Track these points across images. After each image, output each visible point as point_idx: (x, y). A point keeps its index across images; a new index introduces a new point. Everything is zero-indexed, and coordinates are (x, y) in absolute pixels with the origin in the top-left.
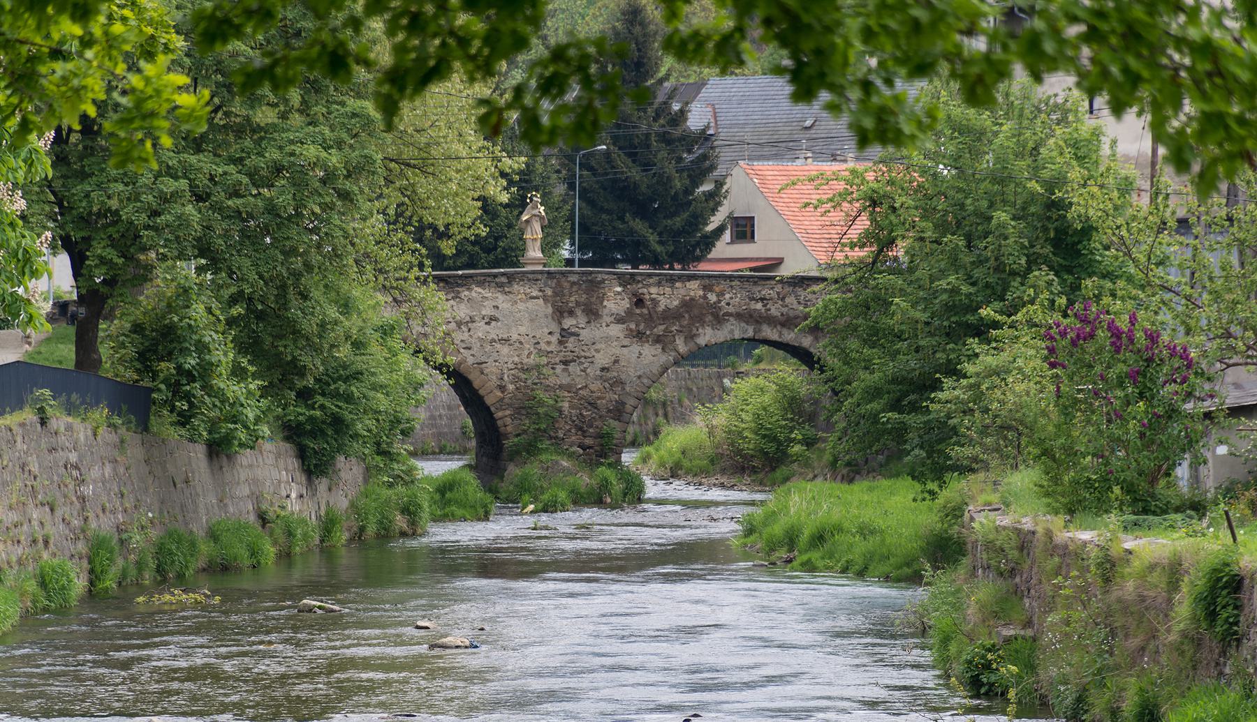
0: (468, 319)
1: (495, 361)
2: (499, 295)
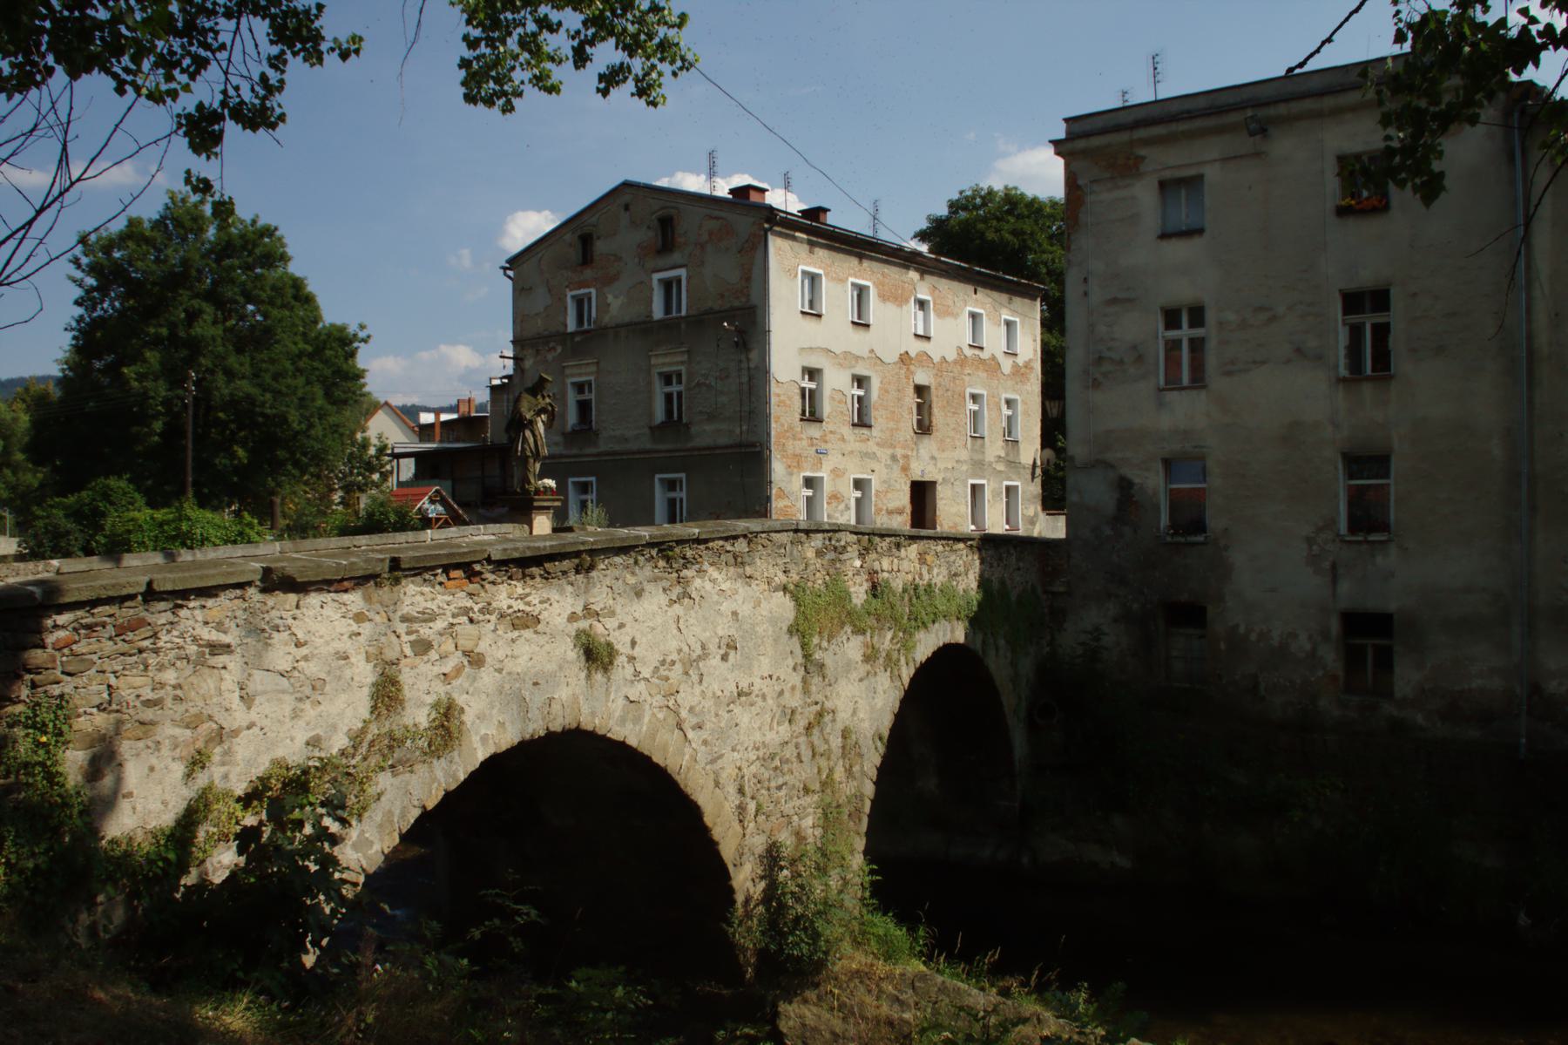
0: (699, 651)
1: (733, 750)
2: (739, 584)
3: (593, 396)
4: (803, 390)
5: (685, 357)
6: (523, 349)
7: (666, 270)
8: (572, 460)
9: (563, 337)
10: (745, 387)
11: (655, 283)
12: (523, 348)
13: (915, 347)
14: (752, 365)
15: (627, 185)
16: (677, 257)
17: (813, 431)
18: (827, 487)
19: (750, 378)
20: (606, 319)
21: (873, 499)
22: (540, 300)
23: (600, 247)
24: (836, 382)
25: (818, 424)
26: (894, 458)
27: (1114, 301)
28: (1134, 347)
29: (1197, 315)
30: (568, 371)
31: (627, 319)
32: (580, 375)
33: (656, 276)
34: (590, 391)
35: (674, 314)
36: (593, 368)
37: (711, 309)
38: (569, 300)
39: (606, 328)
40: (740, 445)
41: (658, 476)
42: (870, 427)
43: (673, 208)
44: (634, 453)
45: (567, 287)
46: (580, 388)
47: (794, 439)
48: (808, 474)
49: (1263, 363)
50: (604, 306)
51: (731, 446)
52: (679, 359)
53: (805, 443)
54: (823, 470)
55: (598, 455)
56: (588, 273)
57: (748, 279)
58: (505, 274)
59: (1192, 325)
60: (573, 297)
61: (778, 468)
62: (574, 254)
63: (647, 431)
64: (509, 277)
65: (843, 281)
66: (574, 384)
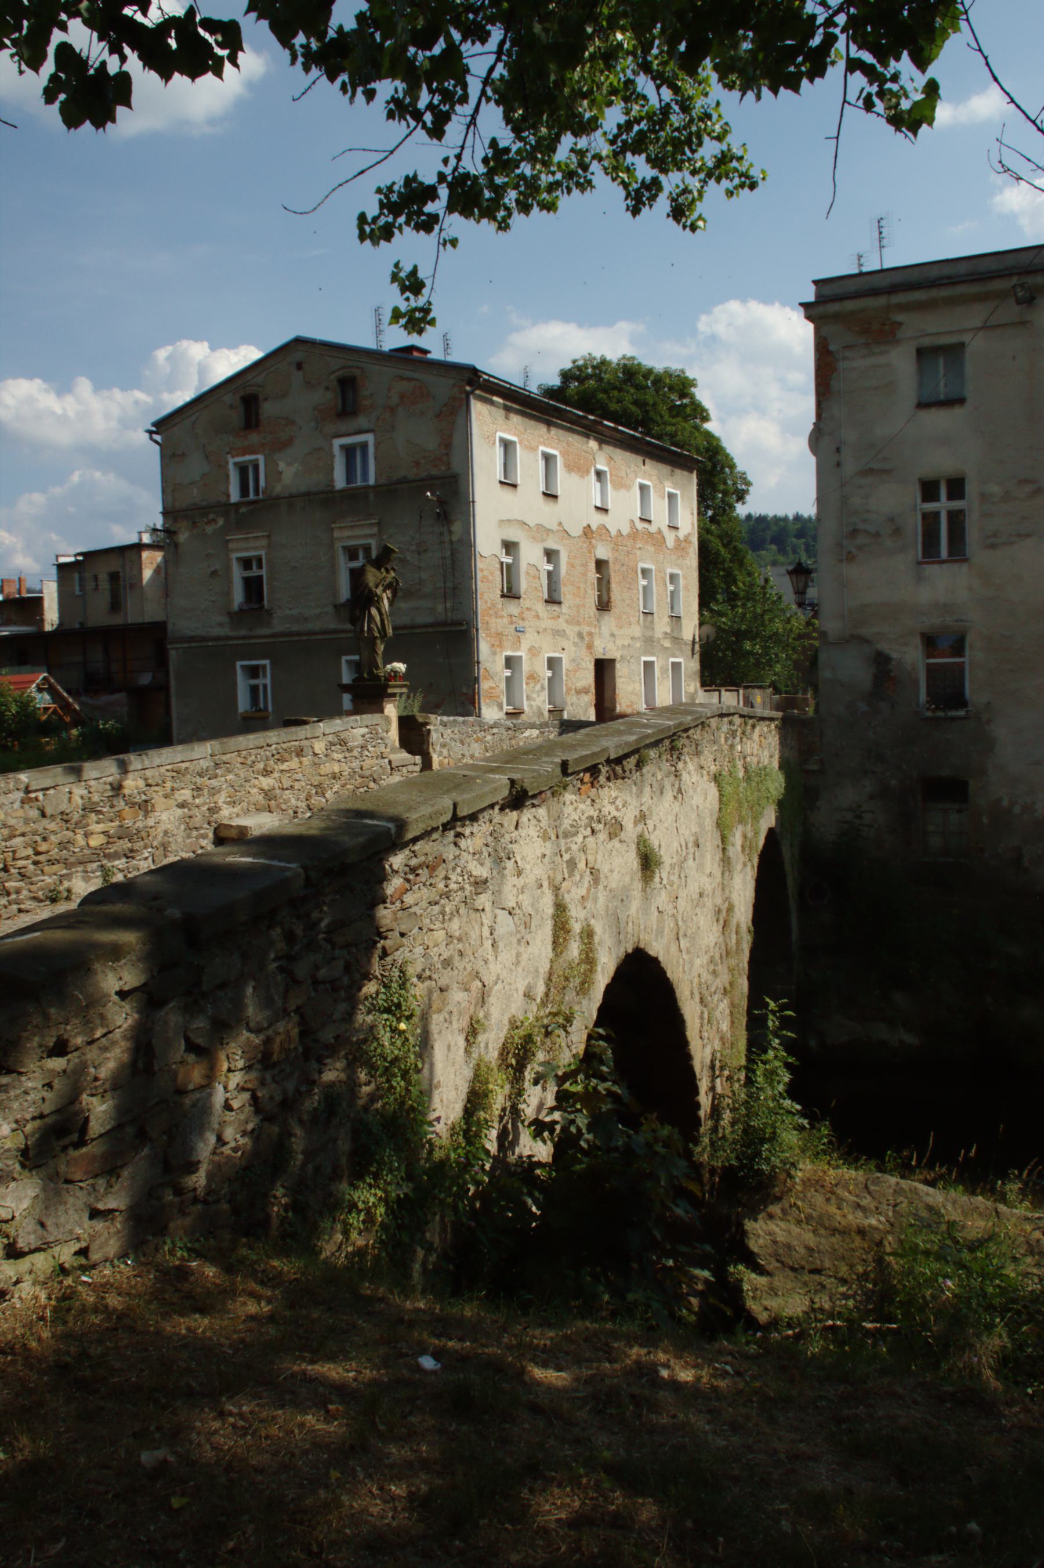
3: (264, 572)
4: (502, 563)
5: (375, 530)
6: (175, 520)
7: (349, 435)
8: (241, 642)
9: (225, 508)
10: (448, 562)
11: (336, 450)
12: (175, 520)
13: (596, 520)
14: (455, 538)
15: (299, 342)
16: (362, 421)
17: (512, 608)
18: (526, 667)
19: (452, 554)
20: (278, 489)
21: (564, 678)
22: (195, 467)
23: (268, 409)
24: (531, 555)
25: (516, 601)
26: (580, 635)
27: (869, 472)
28: (891, 520)
29: (957, 487)
30: (231, 546)
31: (303, 489)
32: (247, 549)
33: (337, 443)
34: (260, 566)
35: (359, 483)
36: (264, 542)
37: (405, 477)
38: (231, 466)
39: (278, 498)
40: (445, 624)
41: (344, 658)
42: (559, 603)
43: (357, 367)
44: (316, 633)
45: (228, 453)
46: (246, 563)
47: (497, 617)
48: (509, 653)
49: (1028, 536)
50: (274, 474)
51: (432, 625)
52: (368, 531)
53: (506, 620)
54: (522, 648)
55: (273, 636)
56: (254, 438)
57: (448, 446)
58: (151, 439)
59: (951, 497)
60: (235, 464)
61: (484, 647)
62: (236, 417)
63: (330, 609)
64: (156, 442)
65: (534, 449)
66: (239, 559)
